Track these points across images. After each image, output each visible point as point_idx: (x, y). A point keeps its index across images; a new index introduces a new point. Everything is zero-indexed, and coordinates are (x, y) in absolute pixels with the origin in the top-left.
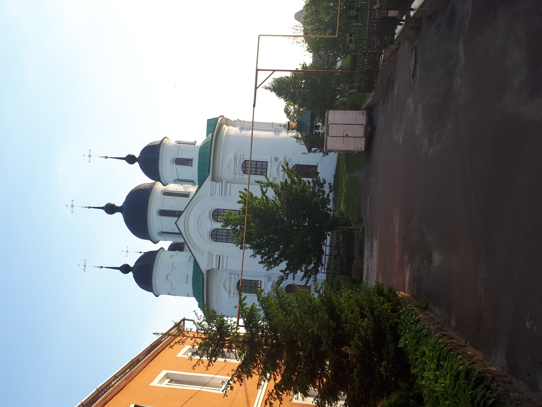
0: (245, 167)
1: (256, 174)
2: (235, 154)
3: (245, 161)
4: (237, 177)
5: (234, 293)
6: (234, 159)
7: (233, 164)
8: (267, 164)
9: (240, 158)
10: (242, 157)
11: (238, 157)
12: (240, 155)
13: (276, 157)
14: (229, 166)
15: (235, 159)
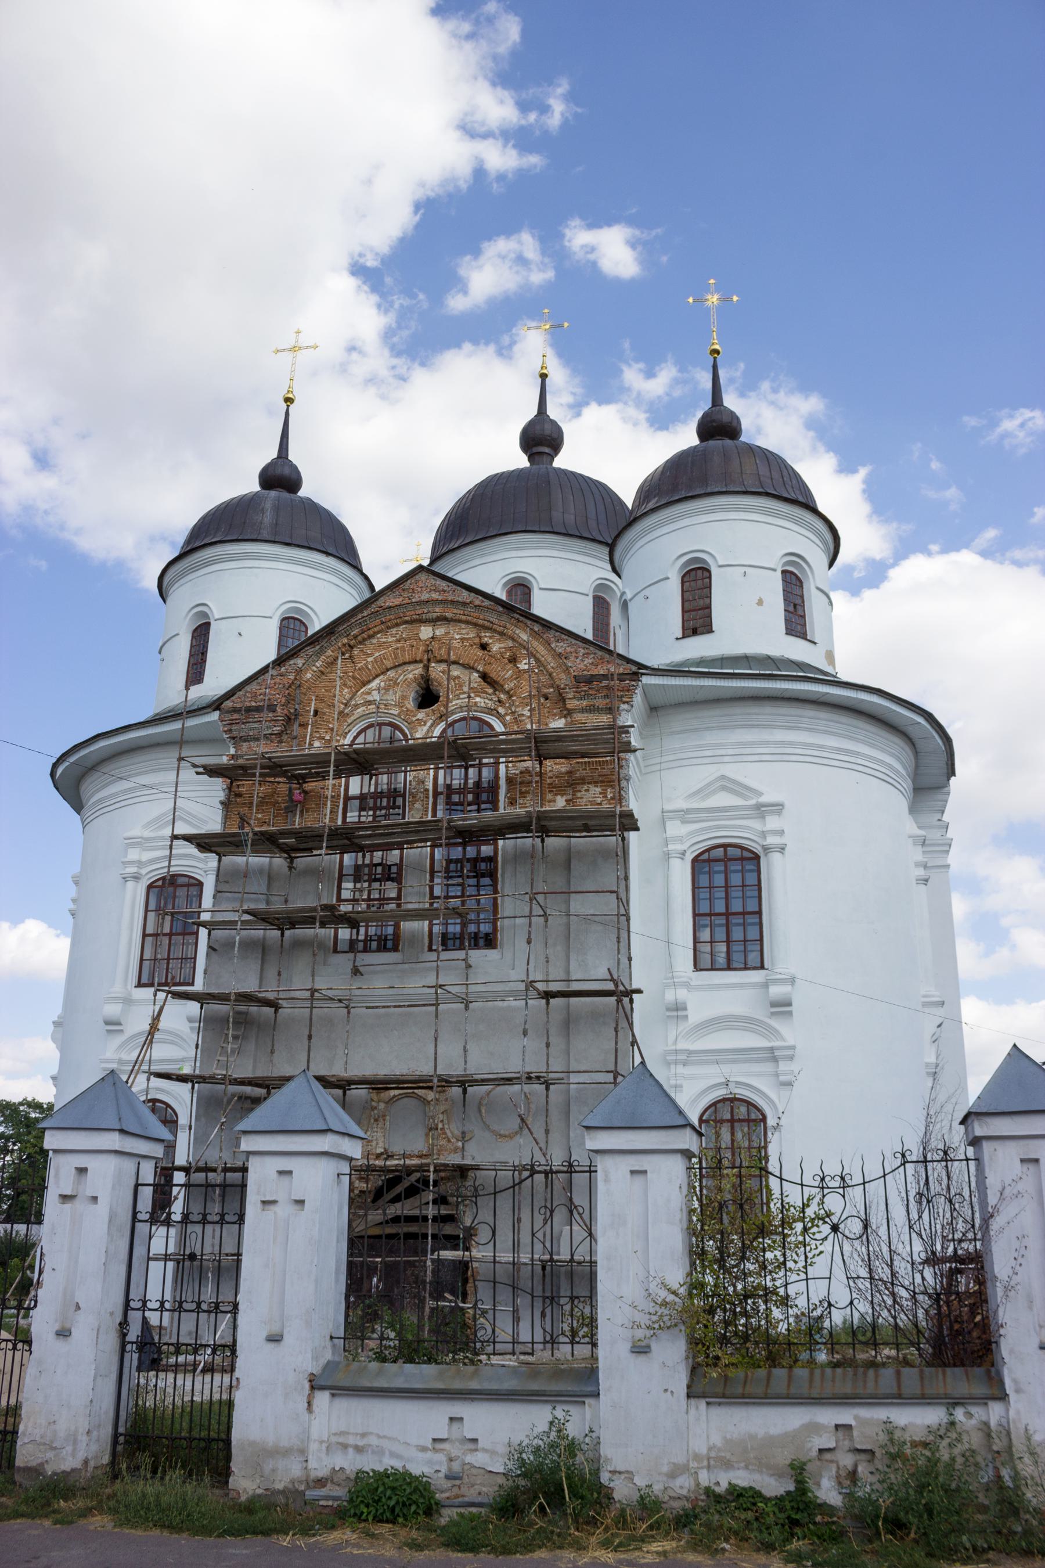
0: (726, 860)
1: (696, 915)
2: (782, 805)
3: (757, 858)
4: (675, 829)
5: (140, 864)
6: (759, 807)
7: (738, 801)
8: (755, 968)
9: (764, 834)
10: (771, 840)
11: (772, 822)
12: (781, 832)
13: (790, 1004)
14: (727, 785)
15: (762, 810)
